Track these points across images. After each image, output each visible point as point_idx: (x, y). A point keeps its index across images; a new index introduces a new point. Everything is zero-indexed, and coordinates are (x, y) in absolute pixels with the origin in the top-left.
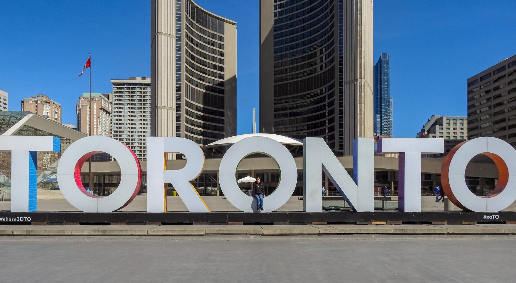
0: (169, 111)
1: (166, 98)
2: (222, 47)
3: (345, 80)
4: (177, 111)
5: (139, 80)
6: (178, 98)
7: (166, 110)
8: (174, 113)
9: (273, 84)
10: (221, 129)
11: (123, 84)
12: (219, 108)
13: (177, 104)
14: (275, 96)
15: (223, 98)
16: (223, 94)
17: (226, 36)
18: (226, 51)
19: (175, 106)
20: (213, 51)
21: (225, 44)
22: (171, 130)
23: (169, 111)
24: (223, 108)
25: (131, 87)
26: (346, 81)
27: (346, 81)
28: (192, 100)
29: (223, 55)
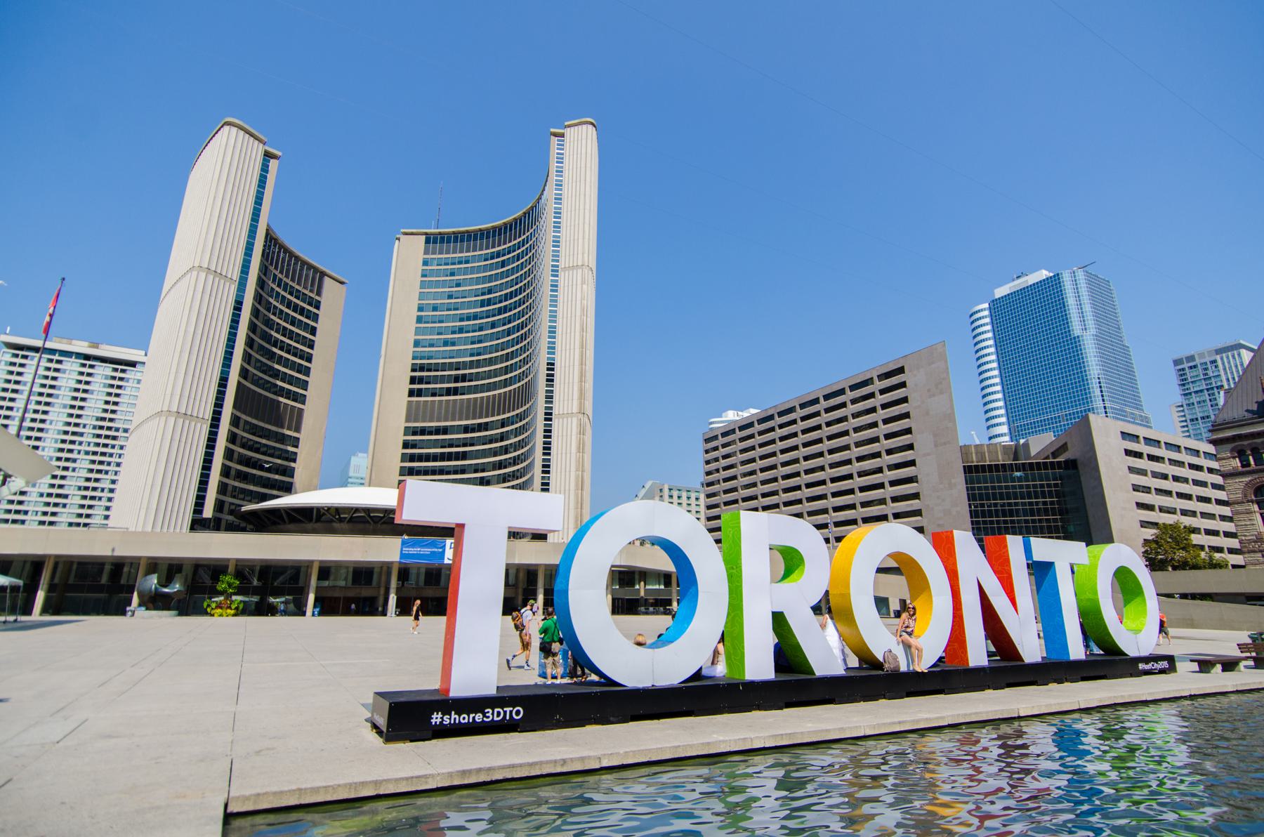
2: (315, 318)
5: (82, 347)
8: (206, 428)
10: (290, 472)
13: (215, 412)
14: (407, 420)
15: (301, 411)
16: (304, 403)
17: (325, 299)
19: (208, 415)
20: (299, 324)
21: (321, 313)
24: (298, 430)
25: (56, 357)
29: (313, 331)
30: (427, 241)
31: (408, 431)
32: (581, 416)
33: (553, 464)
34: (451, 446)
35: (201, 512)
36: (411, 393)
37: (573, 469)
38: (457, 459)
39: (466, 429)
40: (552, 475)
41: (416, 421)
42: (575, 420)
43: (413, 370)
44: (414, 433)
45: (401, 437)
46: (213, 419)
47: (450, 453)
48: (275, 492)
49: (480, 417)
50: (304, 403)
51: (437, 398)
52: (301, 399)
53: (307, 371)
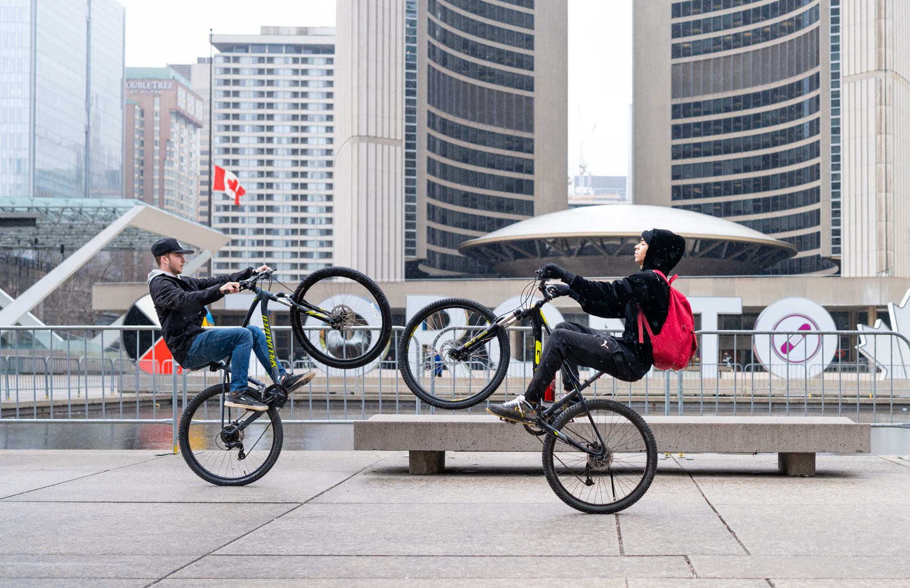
0: (386, 147)
1: (380, 114)
3: (844, 71)
4: (408, 146)
6: (410, 113)
7: (379, 146)
9: (667, 61)
10: (526, 187)
12: (519, 128)
13: (408, 129)
15: (530, 100)
16: (531, 89)
19: (401, 134)
22: (392, 197)
23: (386, 147)
24: (531, 129)
26: (846, 74)
27: (846, 74)
28: (444, 110)
31: (677, 111)
33: (844, 154)
35: (413, 252)
36: (677, 51)
40: (844, 172)
42: (872, 82)
46: (408, 137)
49: (791, 75)
50: (532, 90)
53: (529, 42)
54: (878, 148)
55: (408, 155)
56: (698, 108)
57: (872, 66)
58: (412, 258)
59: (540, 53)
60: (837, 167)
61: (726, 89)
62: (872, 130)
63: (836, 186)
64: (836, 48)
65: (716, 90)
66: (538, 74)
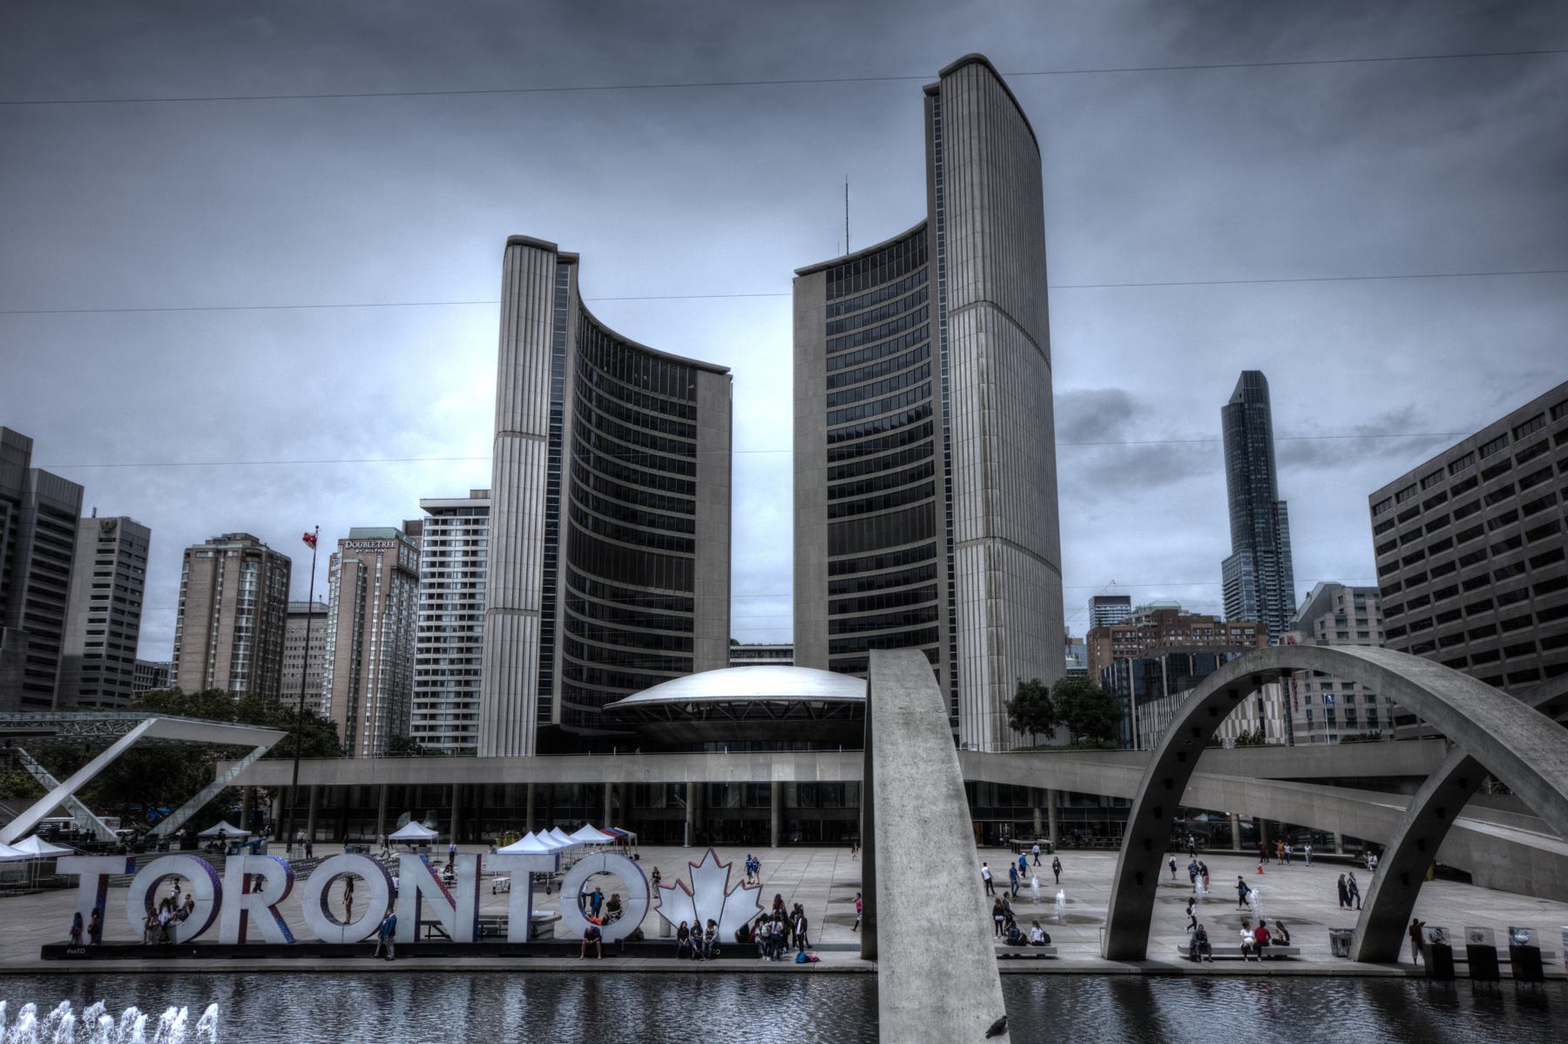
10: (688, 644)
11: (453, 511)
12: (678, 588)
14: (831, 553)
18: (699, 443)
24: (690, 588)
30: (829, 279)
31: (834, 569)
32: (990, 542)
34: (889, 585)
35: (548, 718)
37: (984, 625)
38: (880, 606)
39: (898, 559)
41: (842, 552)
42: (981, 548)
43: (830, 479)
44: (842, 572)
45: (826, 579)
46: (544, 607)
47: (871, 598)
48: (666, 673)
51: (865, 516)
52: (690, 546)
54: (990, 612)
55: (543, 624)
56: (852, 567)
57: (980, 534)
58: (546, 723)
59: (701, 517)
60: (953, 630)
61: (880, 547)
62: (983, 595)
63: (953, 648)
64: (949, 515)
65: (871, 549)
66: (699, 536)
